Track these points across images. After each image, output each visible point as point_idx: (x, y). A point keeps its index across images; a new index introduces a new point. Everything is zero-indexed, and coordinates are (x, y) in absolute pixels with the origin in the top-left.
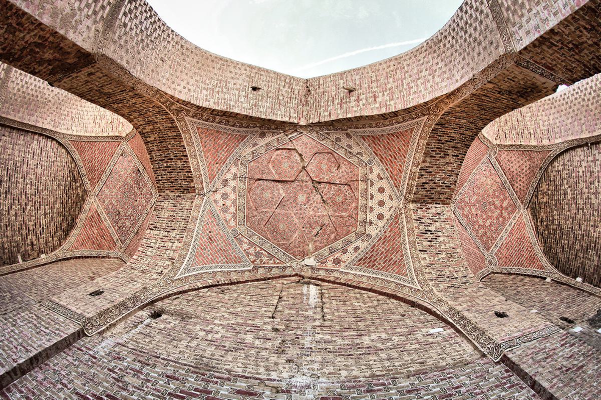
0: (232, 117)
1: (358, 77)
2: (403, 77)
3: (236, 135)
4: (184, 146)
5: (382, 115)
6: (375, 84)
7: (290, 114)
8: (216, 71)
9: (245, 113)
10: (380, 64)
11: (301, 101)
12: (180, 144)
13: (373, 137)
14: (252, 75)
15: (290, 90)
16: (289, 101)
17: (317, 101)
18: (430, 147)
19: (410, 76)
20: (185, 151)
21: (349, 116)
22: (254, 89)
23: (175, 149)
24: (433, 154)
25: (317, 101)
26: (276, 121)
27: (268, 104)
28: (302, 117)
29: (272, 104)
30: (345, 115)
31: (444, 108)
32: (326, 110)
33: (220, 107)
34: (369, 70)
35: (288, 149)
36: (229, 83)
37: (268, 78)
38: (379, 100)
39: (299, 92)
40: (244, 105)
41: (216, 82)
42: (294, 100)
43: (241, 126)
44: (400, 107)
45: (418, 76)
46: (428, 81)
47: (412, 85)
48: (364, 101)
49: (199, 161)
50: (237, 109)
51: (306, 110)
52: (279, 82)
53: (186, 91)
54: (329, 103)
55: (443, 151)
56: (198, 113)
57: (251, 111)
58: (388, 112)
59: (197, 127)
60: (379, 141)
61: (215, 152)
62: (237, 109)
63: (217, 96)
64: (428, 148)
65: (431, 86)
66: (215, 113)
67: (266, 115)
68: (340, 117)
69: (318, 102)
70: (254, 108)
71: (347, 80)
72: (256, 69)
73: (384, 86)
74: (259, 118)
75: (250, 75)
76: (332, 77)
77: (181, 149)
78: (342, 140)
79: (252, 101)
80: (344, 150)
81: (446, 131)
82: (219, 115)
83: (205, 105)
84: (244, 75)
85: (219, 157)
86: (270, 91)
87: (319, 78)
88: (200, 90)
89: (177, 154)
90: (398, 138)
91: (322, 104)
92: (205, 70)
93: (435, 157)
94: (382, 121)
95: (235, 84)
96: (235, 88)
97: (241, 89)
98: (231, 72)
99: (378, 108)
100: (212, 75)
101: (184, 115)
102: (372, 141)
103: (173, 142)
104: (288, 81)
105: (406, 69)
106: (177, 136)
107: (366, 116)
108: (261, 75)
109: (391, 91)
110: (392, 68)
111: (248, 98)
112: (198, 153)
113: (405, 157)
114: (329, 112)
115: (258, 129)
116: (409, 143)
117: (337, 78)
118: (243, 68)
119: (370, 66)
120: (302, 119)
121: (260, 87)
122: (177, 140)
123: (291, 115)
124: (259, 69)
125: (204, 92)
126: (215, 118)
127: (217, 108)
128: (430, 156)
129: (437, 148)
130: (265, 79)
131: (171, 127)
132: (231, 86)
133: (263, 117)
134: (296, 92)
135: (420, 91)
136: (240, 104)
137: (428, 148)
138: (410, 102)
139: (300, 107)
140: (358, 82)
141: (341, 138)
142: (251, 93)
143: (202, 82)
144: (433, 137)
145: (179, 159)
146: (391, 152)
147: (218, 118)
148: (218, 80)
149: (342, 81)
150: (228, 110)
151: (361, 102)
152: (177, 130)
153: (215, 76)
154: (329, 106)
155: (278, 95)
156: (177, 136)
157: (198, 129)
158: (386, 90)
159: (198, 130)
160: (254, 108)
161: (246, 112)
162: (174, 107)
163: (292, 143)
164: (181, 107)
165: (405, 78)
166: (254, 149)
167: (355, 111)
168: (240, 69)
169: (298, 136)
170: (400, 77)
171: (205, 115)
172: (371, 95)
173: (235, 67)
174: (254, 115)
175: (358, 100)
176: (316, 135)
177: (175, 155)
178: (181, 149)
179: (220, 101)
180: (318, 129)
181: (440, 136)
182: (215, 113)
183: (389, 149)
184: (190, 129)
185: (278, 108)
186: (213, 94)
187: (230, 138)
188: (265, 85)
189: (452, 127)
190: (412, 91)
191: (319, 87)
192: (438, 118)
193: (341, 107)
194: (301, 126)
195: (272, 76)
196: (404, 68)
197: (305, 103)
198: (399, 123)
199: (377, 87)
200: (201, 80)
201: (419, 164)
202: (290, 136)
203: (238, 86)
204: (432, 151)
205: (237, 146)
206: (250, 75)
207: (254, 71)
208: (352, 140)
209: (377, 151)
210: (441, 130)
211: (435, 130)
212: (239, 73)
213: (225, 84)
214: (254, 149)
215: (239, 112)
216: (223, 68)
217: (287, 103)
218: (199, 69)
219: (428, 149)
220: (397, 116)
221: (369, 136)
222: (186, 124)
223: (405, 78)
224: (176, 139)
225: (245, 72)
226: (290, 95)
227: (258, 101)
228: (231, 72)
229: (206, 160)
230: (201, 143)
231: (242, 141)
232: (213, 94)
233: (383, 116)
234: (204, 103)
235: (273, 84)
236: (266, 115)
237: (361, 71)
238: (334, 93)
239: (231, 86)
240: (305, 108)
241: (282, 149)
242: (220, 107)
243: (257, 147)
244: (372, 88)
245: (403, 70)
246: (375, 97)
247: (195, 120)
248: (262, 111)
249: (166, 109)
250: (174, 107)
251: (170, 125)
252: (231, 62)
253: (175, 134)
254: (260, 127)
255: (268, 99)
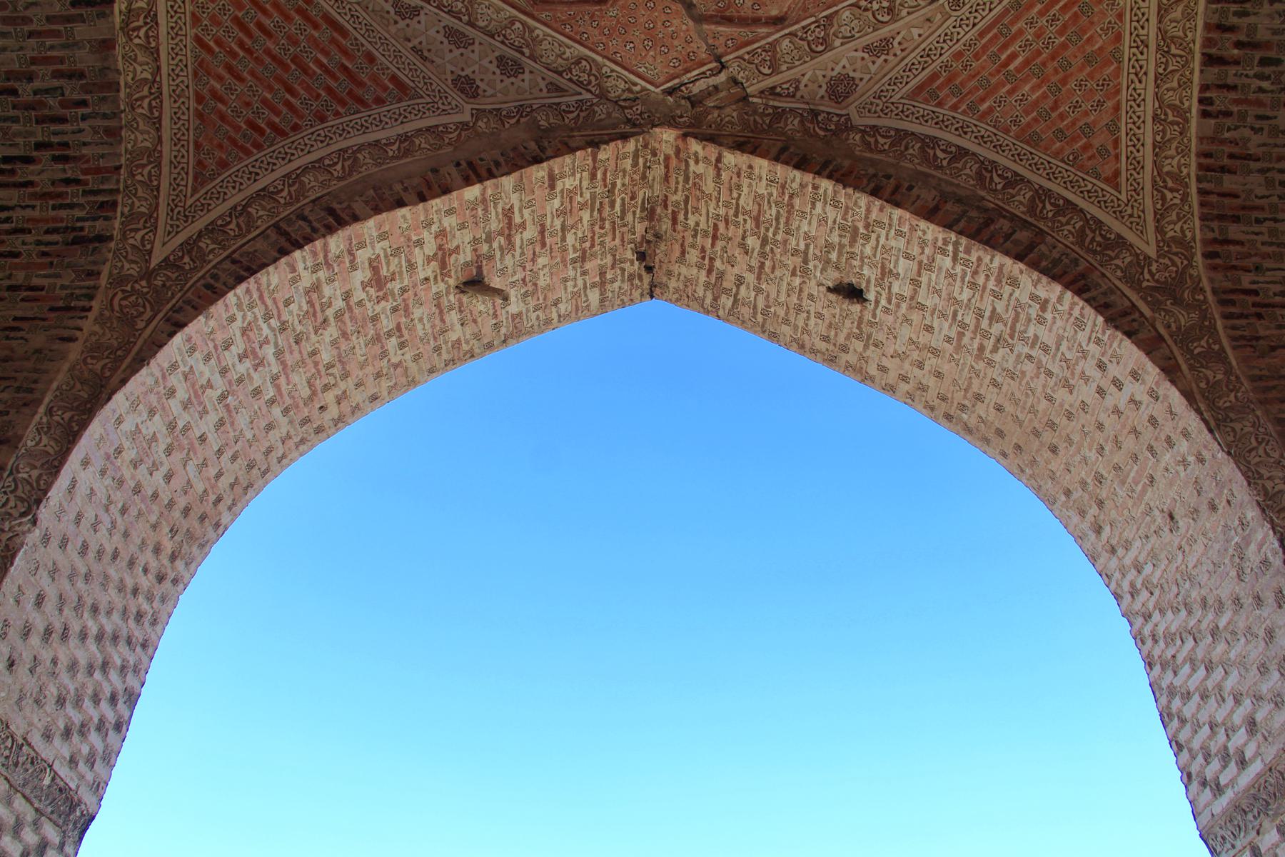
0: (959, 200)
1: (453, 336)
2: (283, 380)
3: (954, 108)
4: (1205, 114)
5: (342, 223)
6: (387, 323)
7: (719, 175)
8: (992, 396)
9: (897, 212)
10: (374, 398)
11: (674, 221)
12: (1219, 129)
13: (361, 101)
14: (858, 345)
15: (718, 264)
16: (722, 226)
17: (607, 225)
18: (99, 122)
19: (257, 392)
20: (1204, 88)
21: (472, 192)
22: (853, 293)
23: (1259, 103)
24: (72, 91)
25: (607, 225)
26: (776, 159)
27: (805, 228)
28: (667, 158)
29: (787, 223)
30: (489, 192)
31: (97, 328)
32: (571, 194)
33: (996, 264)
34: (413, 368)
35: (729, 20)
36: (948, 340)
37: (801, 324)
38: (361, 275)
39: (683, 253)
40: (900, 243)
41: (997, 357)
42: (703, 226)
43: (929, 143)
44: (273, 276)
45: (227, 406)
46: (186, 406)
47: (243, 368)
48: (418, 256)
49: (1154, 20)
50: (929, 236)
51: (651, 187)
52: (761, 305)
53: (1113, 370)
54: (558, 223)
55: (28, 107)
56: (1095, 252)
57: (874, 216)
58: (318, 244)
59: (1117, 187)
60: (329, 90)
61: (1064, 46)
62: (929, 236)
63: (1000, 306)
64: (105, 116)
65: (171, 393)
66: (1023, 236)
67: (815, 187)
68: (508, 182)
69: (603, 220)
70: (861, 225)
71: (495, 315)
72: (843, 363)
73: (350, 327)
74: (843, 177)
75: (866, 347)
76: (554, 315)
77: (1222, 100)
78: (493, 67)
79: (868, 250)
80: (481, 24)
81: (52, 213)
82: (1013, 218)
83: (1052, 291)
84: (890, 351)
85: (1054, 19)
86: (794, 274)
87: (604, 305)
88: (1063, 348)
89: (1257, 76)
90: (252, 125)
91: (586, 215)
92: (1033, 410)
93: (58, 75)
94: (335, 185)
95: (929, 329)
96: (928, 315)
97: (904, 306)
98: (938, 375)
99: (362, 245)
100: (1009, 385)
101: (1154, 268)
102: (361, 84)
103: (1256, 139)
104: (726, 301)
105: (277, 411)
106: (1223, 169)
107: (401, 204)
108: (825, 339)
109: (320, 320)
110: (330, 397)
111: (883, 267)
112: (1151, 61)
113: (198, 40)
114: (558, 189)
115: (858, 120)
116: (200, 115)
117: (534, 316)
118: (892, 377)
119: (412, 383)
120: (671, 152)
121: (833, 297)
122: (1227, 149)
123: (711, 172)
124: (831, 360)
125: (1046, 336)
126: (1032, 209)
127: (1008, 261)
128: (82, 75)
129: (63, 120)
130: (812, 321)
131: (1236, 219)
132: (945, 328)
133: (826, 185)
134: (693, 256)
135: (207, 358)
136: (915, 251)
137: (105, 116)
138: (239, 306)
139: (678, 197)
140: (453, 317)
141: (498, 77)
142: (868, 282)
143: (1049, 373)
144: (98, 170)
145: (1254, 46)
146: (268, 52)
147: (1019, 204)
148: (990, 363)
149: (513, 308)
150: (964, 241)
151: (430, 247)
152: (1213, 199)
153: (999, 380)
154: (561, 213)
155: (763, 255)
156: (1223, 169)
157: (1113, 180)
158: (339, 316)
159: (1117, 174)
160: (861, 225)
161: (895, 217)
162: (1185, 319)
163: (711, 48)
164: (1156, 306)
165: (275, 378)
166: (885, 32)
167: (450, 212)
168: (904, 379)
169: (685, 79)
170: (295, 378)
171: (1066, 235)
172: (396, 286)
173: (923, 388)
174: (863, 200)
175: (442, 257)
176: (610, 83)
177: (1267, 70)
178: (1222, 100)
179: (991, 284)
180: (601, 111)
181: (68, 182)
182: (1023, 236)
183: (281, 63)
184: (1148, 187)
185: (766, 207)
186: (1016, 320)
187: (983, 100)
188: (811, 297)
189: (28, 238)
190: (239, 346)
191: (602, 274)
192: (105, 270)
193: (510, 219)
194: (671, 122)
195: (786, 329)
196: (286, 411)
197: (659, 210)
198: (264, 194)
199: (375, 319)
200: (1051, 382)
201: (126, 23)
202: (722, 77)
203: (915, 317)
204: (83, 103)
205: (958, 55)
206: (866, 347)
207: (851, 358)
208: (449, 67)
209: (333, 41)
210: (78, 213)
211: (102, 205)
212: (907, 365)
213: (966, 340)
214: (885, 32)
215: (923, 224)
216: (965, 397)
217: (731, 217)
218: (1052, 425)
219: (105, 109)
220: (276, 226)
221: (380, 101)
222: (1159, 217)
223: (275, 378)
224: (1231, 156)
225: (885, 362)
226: (718, 248)
227: (841, 246)
228: (938, 375)
229: (1120, 16)
230: (1117, 108)
231: (934, 77)
232: (1016, 320)
233: (337, 217)
234: (1054, 298)
235: (782, 298)
236: (815, 187)
237: (445, 356)
238: (542, 261)
239: (945, 328)
240: (658, 190)
241: (756, 21)
242: (996, 264)
243: (873, 37)
244: (395, 310)
245: (288, 401)
246: (378, 281)
247: (1117, 227)
248: (829, 208)
249: (1219, 324)
250: (1185, 319)
251: (1234, 231)
252: (932, 409)
253: (1229, 183)
254: (846, 126)
255: (802, 247)
